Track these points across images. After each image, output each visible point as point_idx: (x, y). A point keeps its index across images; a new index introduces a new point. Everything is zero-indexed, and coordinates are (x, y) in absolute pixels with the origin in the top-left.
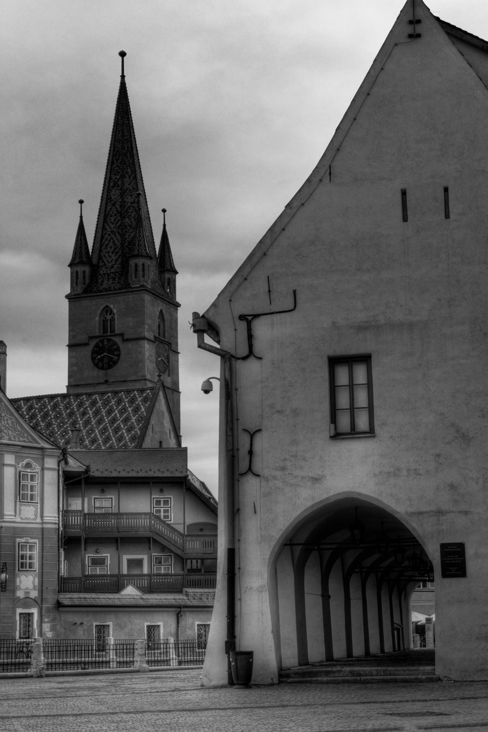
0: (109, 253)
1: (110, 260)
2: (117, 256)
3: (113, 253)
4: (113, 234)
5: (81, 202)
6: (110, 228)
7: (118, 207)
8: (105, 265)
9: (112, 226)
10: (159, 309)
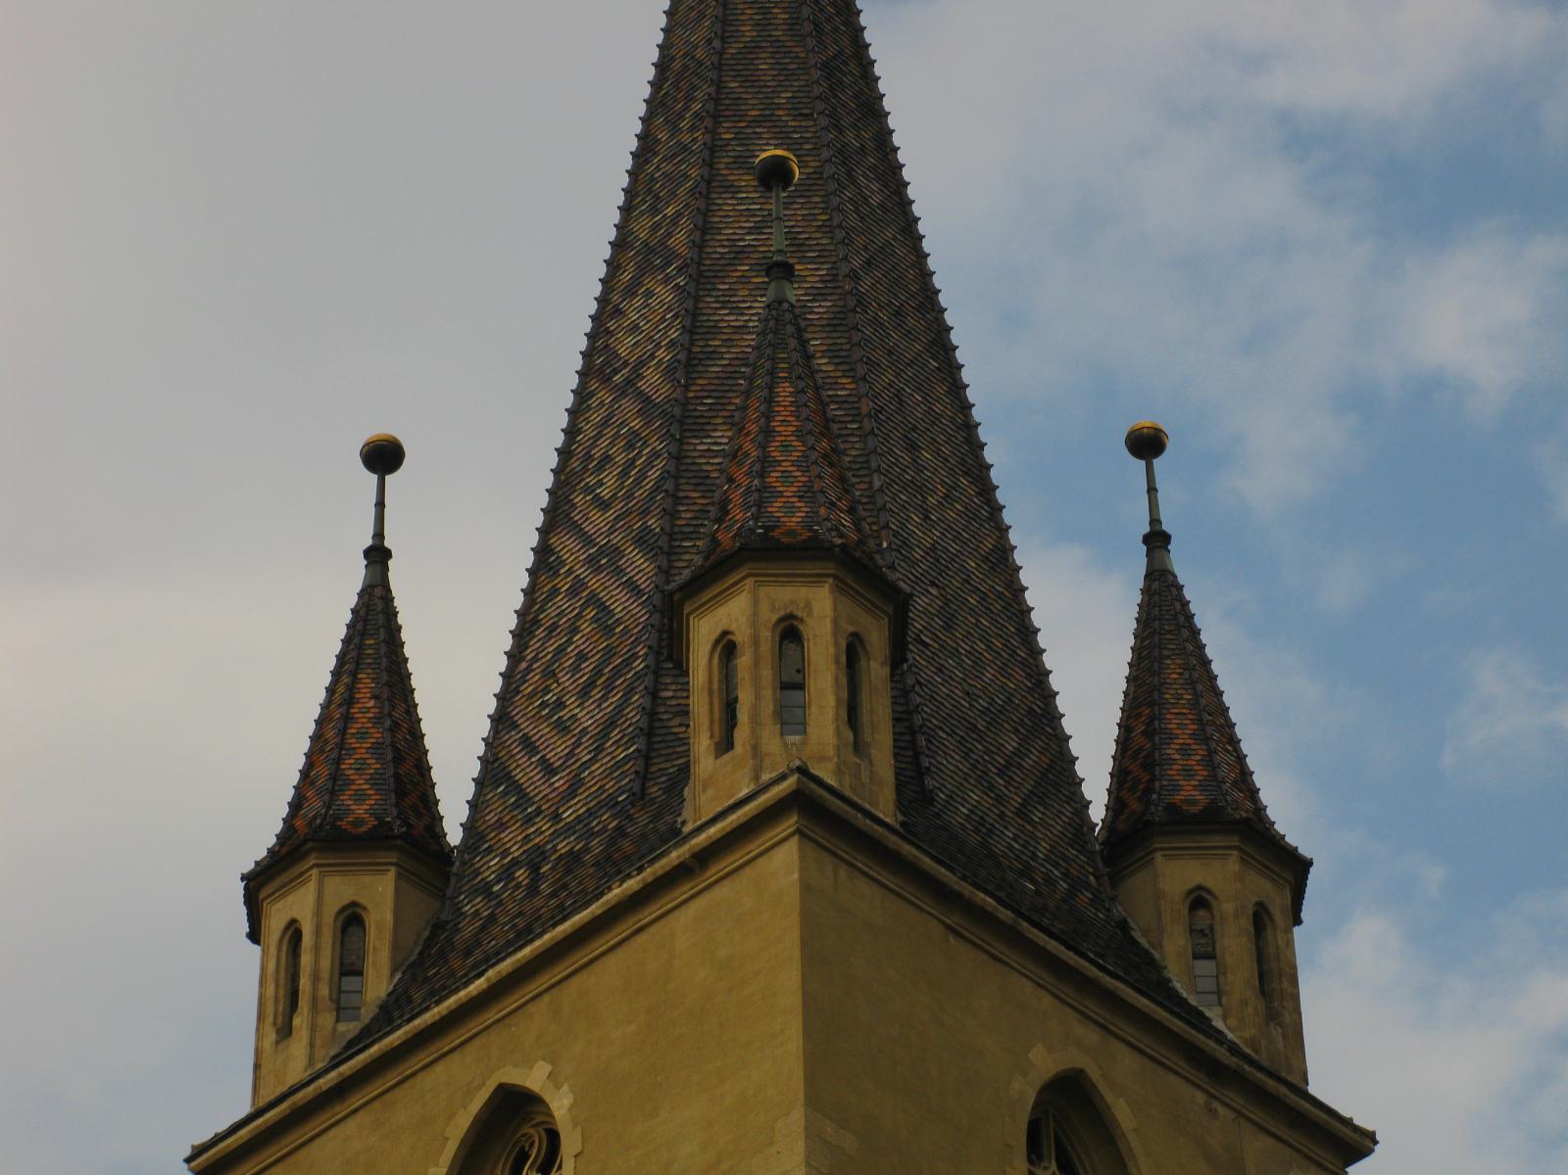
0: (560, 705)
1: (556, 749)
2: (615, 698)
3: (584, 693)
4: (598, 570)
5: (383, 457)
6: (588, 541)
7: (652, 381)
8: (524, 798)
9: (597, 522)
10: (1045, 1063)
